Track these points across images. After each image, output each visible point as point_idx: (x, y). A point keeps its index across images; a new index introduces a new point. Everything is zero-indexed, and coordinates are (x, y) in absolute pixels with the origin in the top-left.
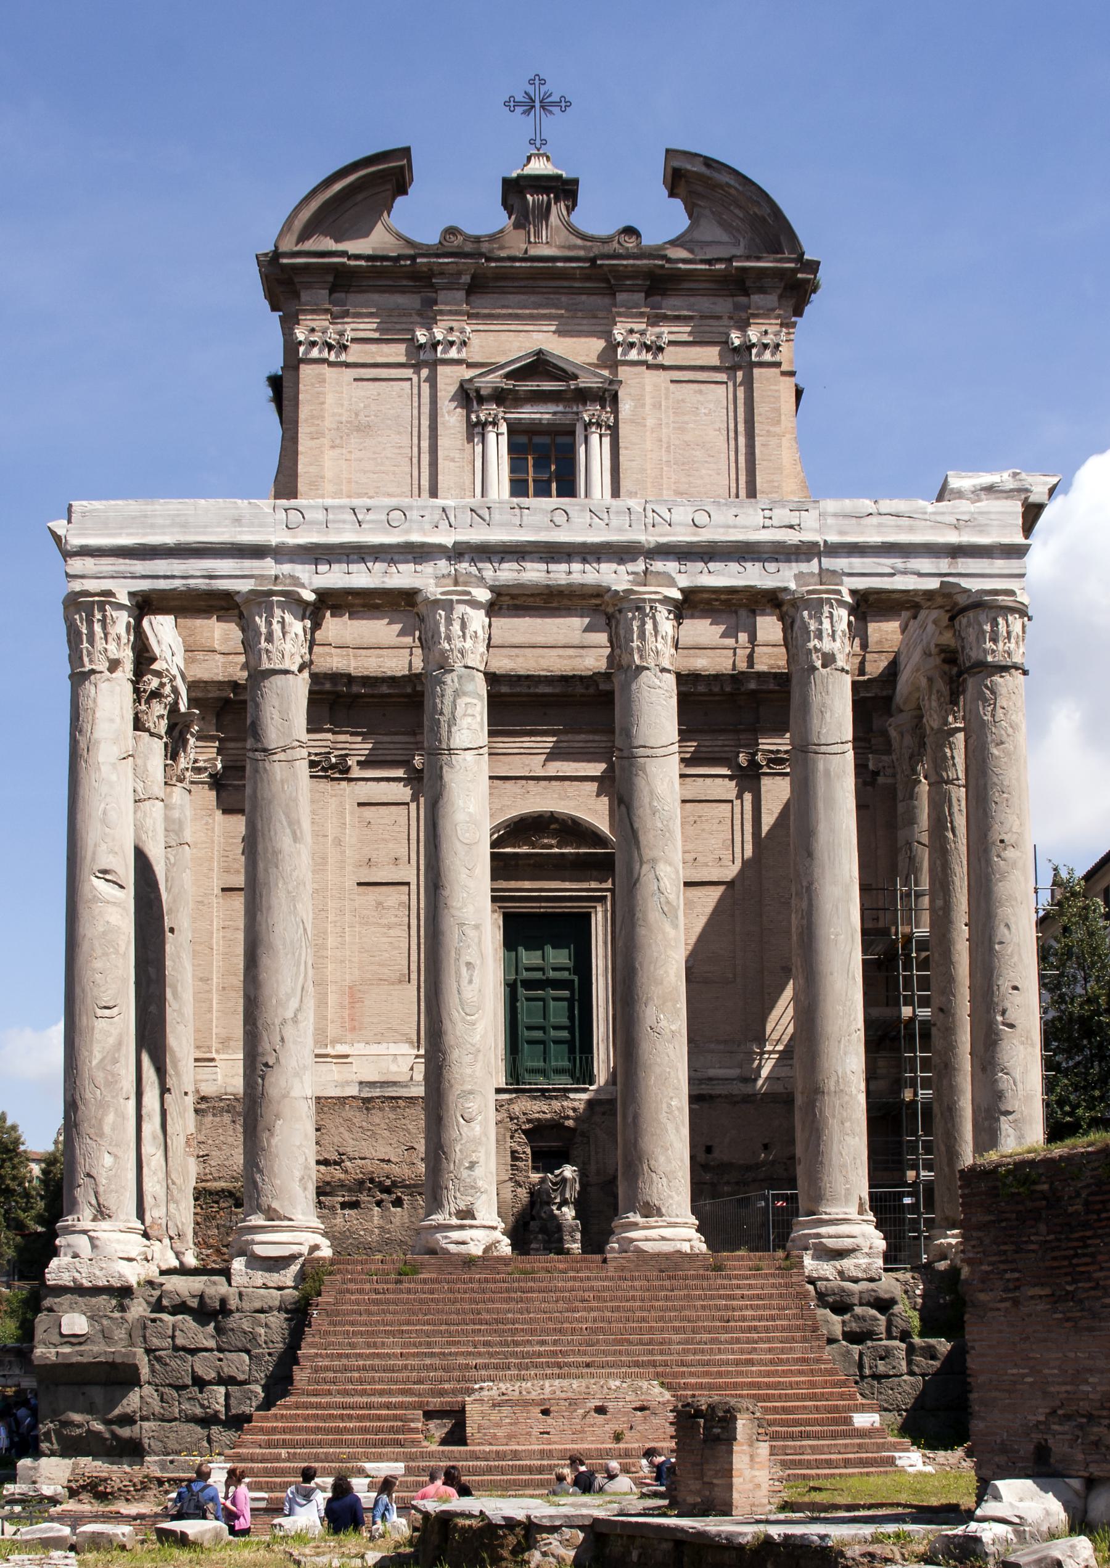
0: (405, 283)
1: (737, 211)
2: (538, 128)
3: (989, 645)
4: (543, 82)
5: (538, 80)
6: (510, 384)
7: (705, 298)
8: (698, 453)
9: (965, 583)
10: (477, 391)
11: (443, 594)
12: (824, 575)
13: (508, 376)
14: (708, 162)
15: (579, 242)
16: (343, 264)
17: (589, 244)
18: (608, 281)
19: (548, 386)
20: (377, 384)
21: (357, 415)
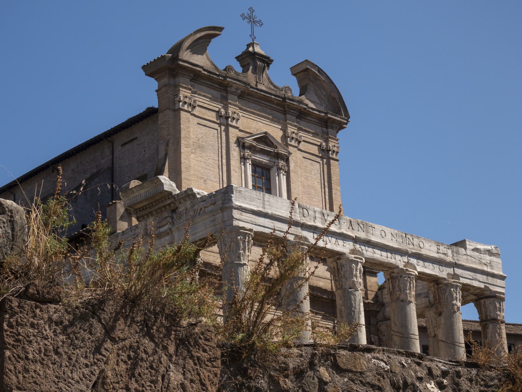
0: (216, 86)
1: (323, 92)
2: (252, 31)
3: (498, 313)
4: (253, 11)
5: (252, 10)
6: (254, 144)
7: (313, 125)
8: (312, 191)
9: (492, 288)
10: (244, 143)
11: (355, 258)
12: (456, 276)
13: (255, 140)
14: (320, 70)
15: (272, 87)
16: (199, 71)
17: (276, 89)
18: (279, 107)
19: (267, 148)
20: (205, 128)
21: (199, 140)
